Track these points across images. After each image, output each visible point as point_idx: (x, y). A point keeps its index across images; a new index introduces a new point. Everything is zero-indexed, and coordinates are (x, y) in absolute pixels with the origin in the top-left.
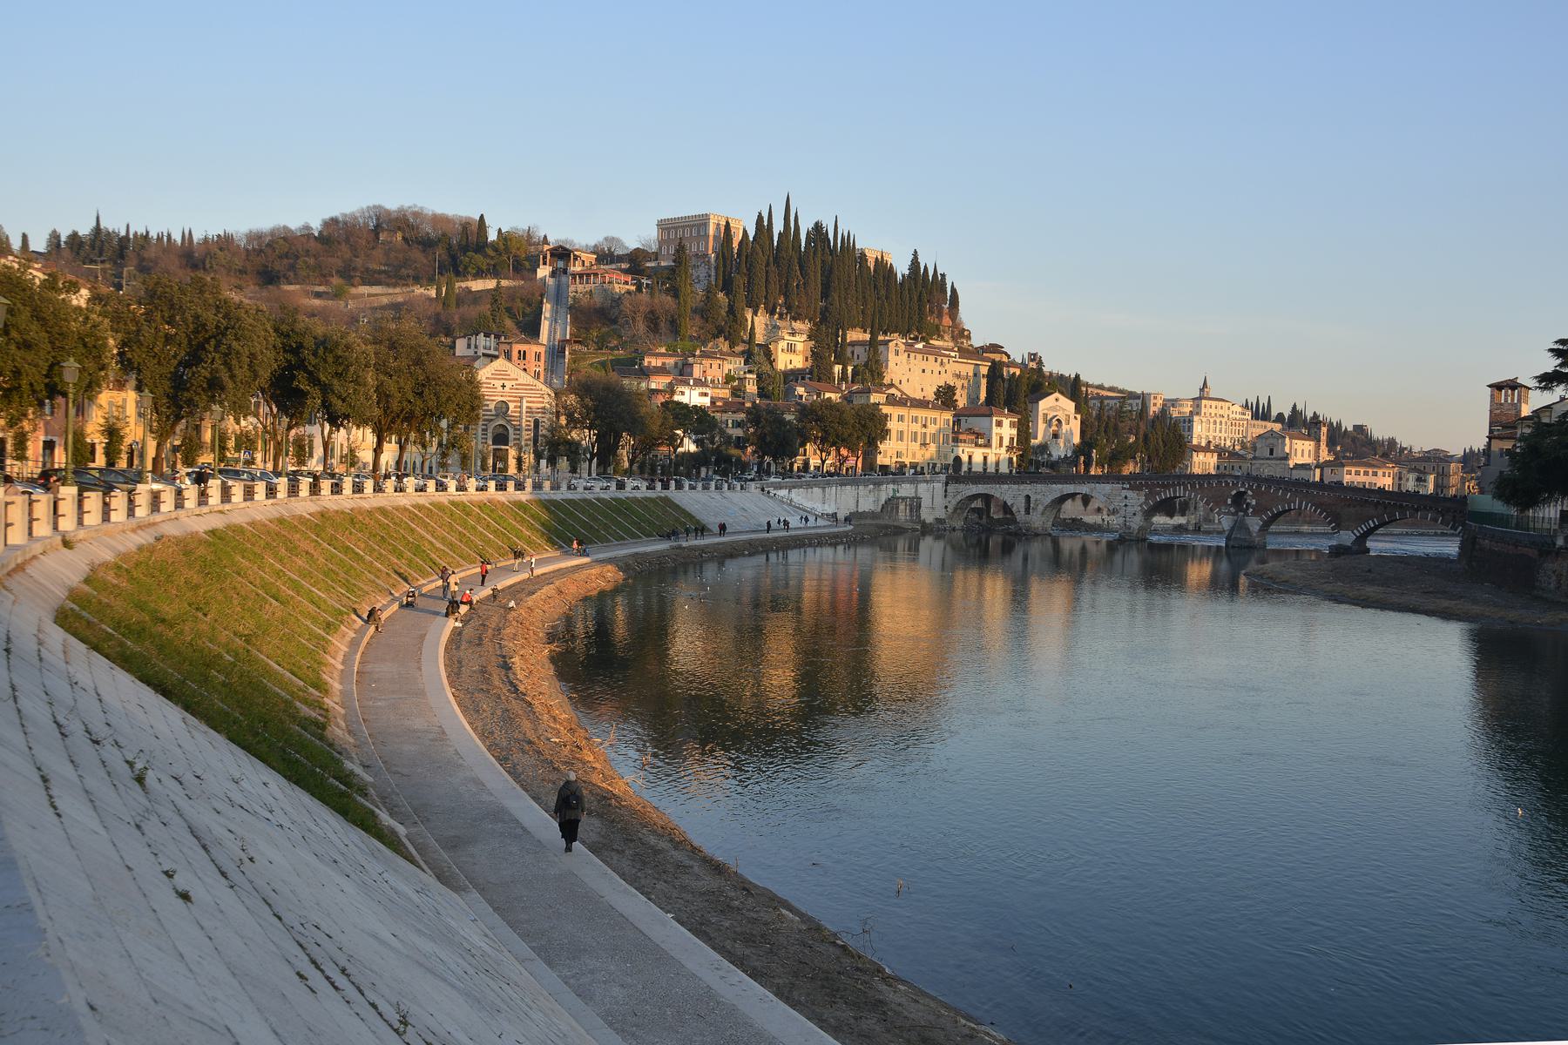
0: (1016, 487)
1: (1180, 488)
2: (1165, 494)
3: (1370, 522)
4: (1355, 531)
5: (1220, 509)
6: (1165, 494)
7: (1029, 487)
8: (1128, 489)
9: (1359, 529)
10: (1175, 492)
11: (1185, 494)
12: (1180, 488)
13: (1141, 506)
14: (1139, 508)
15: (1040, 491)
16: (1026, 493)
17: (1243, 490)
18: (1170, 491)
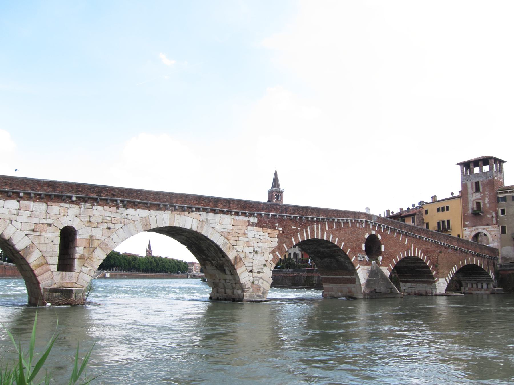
0: (40, 207)
1: (317, 228)
2: (302, 235)
3: (454, 268)
4: (447, 278)
5: (356, 257)
6: (302, 235)
7: (73, 210)
8: (258, 225)
9: (449, 275)
10: (312, 232)
11: (322, 235)
12: (317, 228)
13: (273, 252)
14: (271, 256)
15: (99, 220)
16: (65, 222)
17: (373, 233)
18: (307, 231)
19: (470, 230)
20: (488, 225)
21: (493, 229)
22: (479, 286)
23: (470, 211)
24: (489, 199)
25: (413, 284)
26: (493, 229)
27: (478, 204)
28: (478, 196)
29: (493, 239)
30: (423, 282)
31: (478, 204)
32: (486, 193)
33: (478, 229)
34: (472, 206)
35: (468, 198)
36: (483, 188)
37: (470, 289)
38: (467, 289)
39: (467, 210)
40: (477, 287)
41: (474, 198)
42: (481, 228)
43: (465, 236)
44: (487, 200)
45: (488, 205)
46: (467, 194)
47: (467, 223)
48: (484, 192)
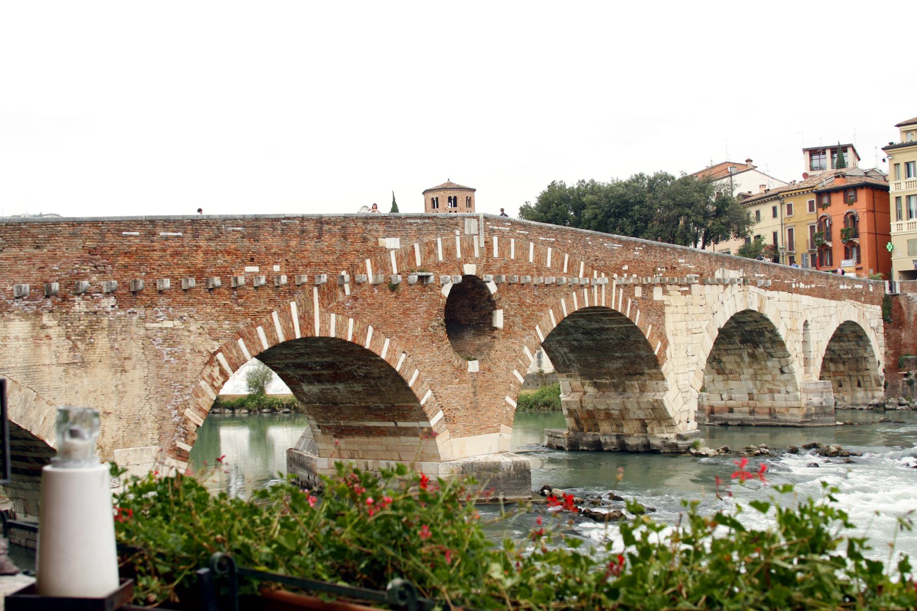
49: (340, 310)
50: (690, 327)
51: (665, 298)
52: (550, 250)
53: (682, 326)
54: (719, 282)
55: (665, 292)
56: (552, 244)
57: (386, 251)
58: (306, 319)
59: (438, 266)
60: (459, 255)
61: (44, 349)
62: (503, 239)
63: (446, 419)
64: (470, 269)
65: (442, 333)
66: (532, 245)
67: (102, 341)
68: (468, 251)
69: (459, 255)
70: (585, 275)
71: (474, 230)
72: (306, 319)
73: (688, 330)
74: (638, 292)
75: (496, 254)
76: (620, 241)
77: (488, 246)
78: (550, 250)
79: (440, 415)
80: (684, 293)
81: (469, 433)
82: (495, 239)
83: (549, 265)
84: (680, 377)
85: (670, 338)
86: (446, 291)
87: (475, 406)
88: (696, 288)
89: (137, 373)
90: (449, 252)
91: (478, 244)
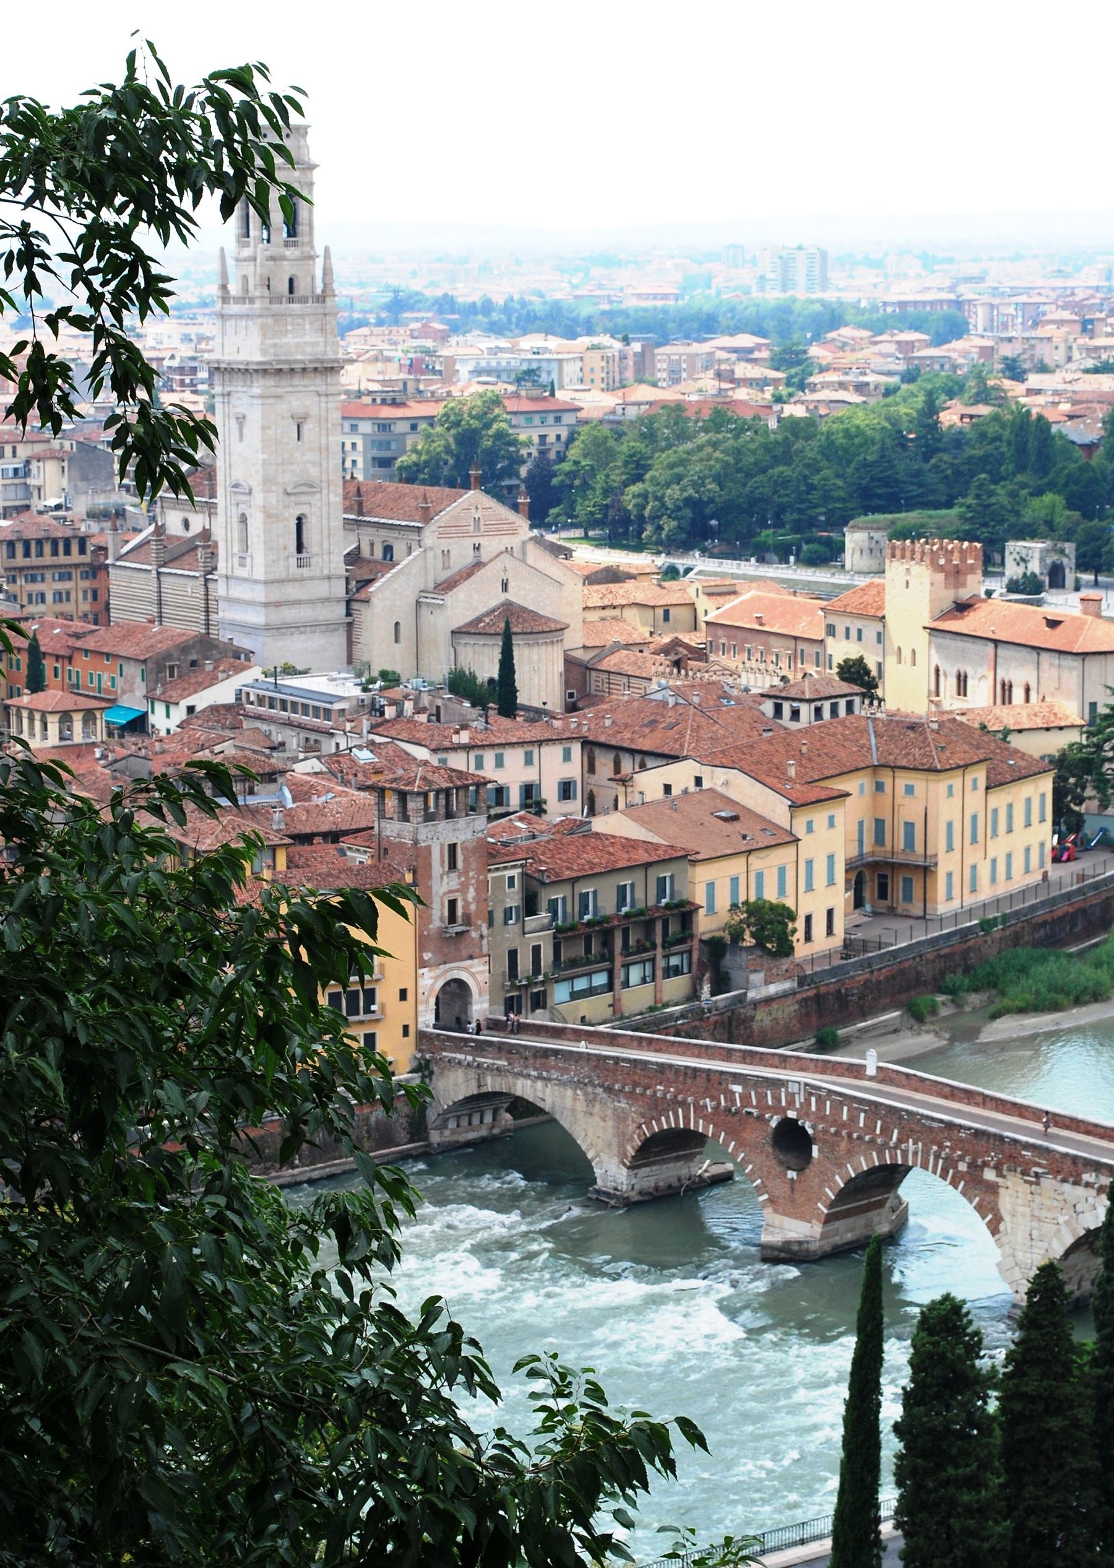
19: (432, 974)
20: (471, 957)
21: (481, 968)
22: (476, 1120)
23: (436, 924)
24: (476, 890)
25: (654, 1168)
26: (481, 968)
27: (452, 904)
28: (453, 882)
29: (480, 994)
30: (678, 1159)
31: (452, 904)
32: (471, 874)
33: (452, 969)
34: (438, 911)
35: (430, 887)
36: (465, 860)
37: (453, 1132)
38: (447, 1133)
39: (430, 920)
40: (470, 1123)
41: (445, 889)
42: (458, 968)
43: (420, 991)
44: (471, 893)
45: (473, 907)
46: (430, 877)
47: (427, 956)
48: (466, 872)
49: (707, 1119)
50: (1037, 1213)
51: (1000, 1180)
52: (862, 1115)
53: (1028, 1210)
54: (1088, 1185)
55: (1000, 1175)
56: (865, 1111)
57: (733, 1093)
58: (686, 1118)
59: (768, 1108)
60: (784, 1103)
61: (578, 1104)
62: (820, 1101)
63: (771, 1201)
64: (792, 1114)
65: (770, 1150)
66: (845, 1109)
67: (598, 1106)
68: (791, 1103)
69: (784, 1103)
70: (900, 1141)
71: (796, 1090)
72: (686, 1118)
73: (1032, 1216)
74: (963, 1167)
75: (813, 1108)
76: (941, 1121)
77: (808, 1102)
78: (862, 1115)
79: (766, 1196)
80: (1030, 1183)
81: (785, 1214)
82: (813, 1099)
83: (861, 1124)
84: (1020, 1255)
85: (1007, 1217)
86: (773, 1124)
87: (793, 1201)
88: (1048, 1182)
89: (610, 1123)
90: (777, 1099)
91: (799, 1100)
